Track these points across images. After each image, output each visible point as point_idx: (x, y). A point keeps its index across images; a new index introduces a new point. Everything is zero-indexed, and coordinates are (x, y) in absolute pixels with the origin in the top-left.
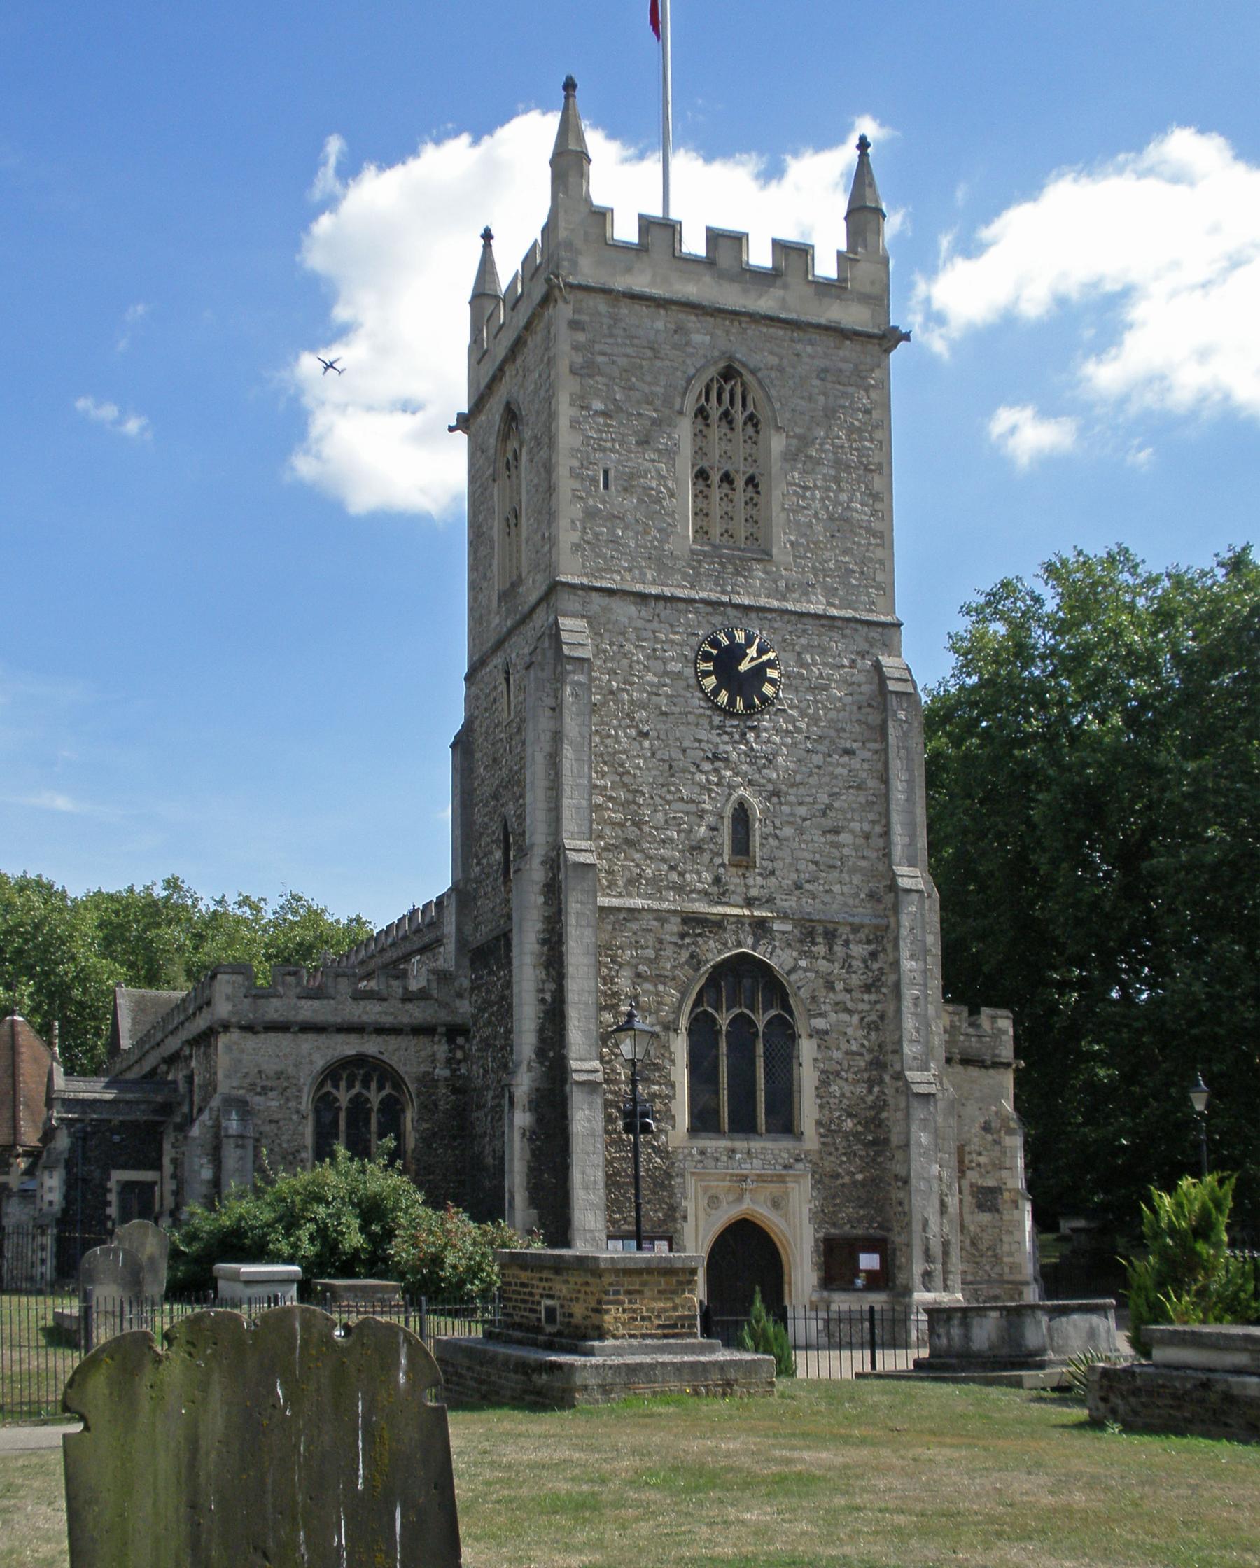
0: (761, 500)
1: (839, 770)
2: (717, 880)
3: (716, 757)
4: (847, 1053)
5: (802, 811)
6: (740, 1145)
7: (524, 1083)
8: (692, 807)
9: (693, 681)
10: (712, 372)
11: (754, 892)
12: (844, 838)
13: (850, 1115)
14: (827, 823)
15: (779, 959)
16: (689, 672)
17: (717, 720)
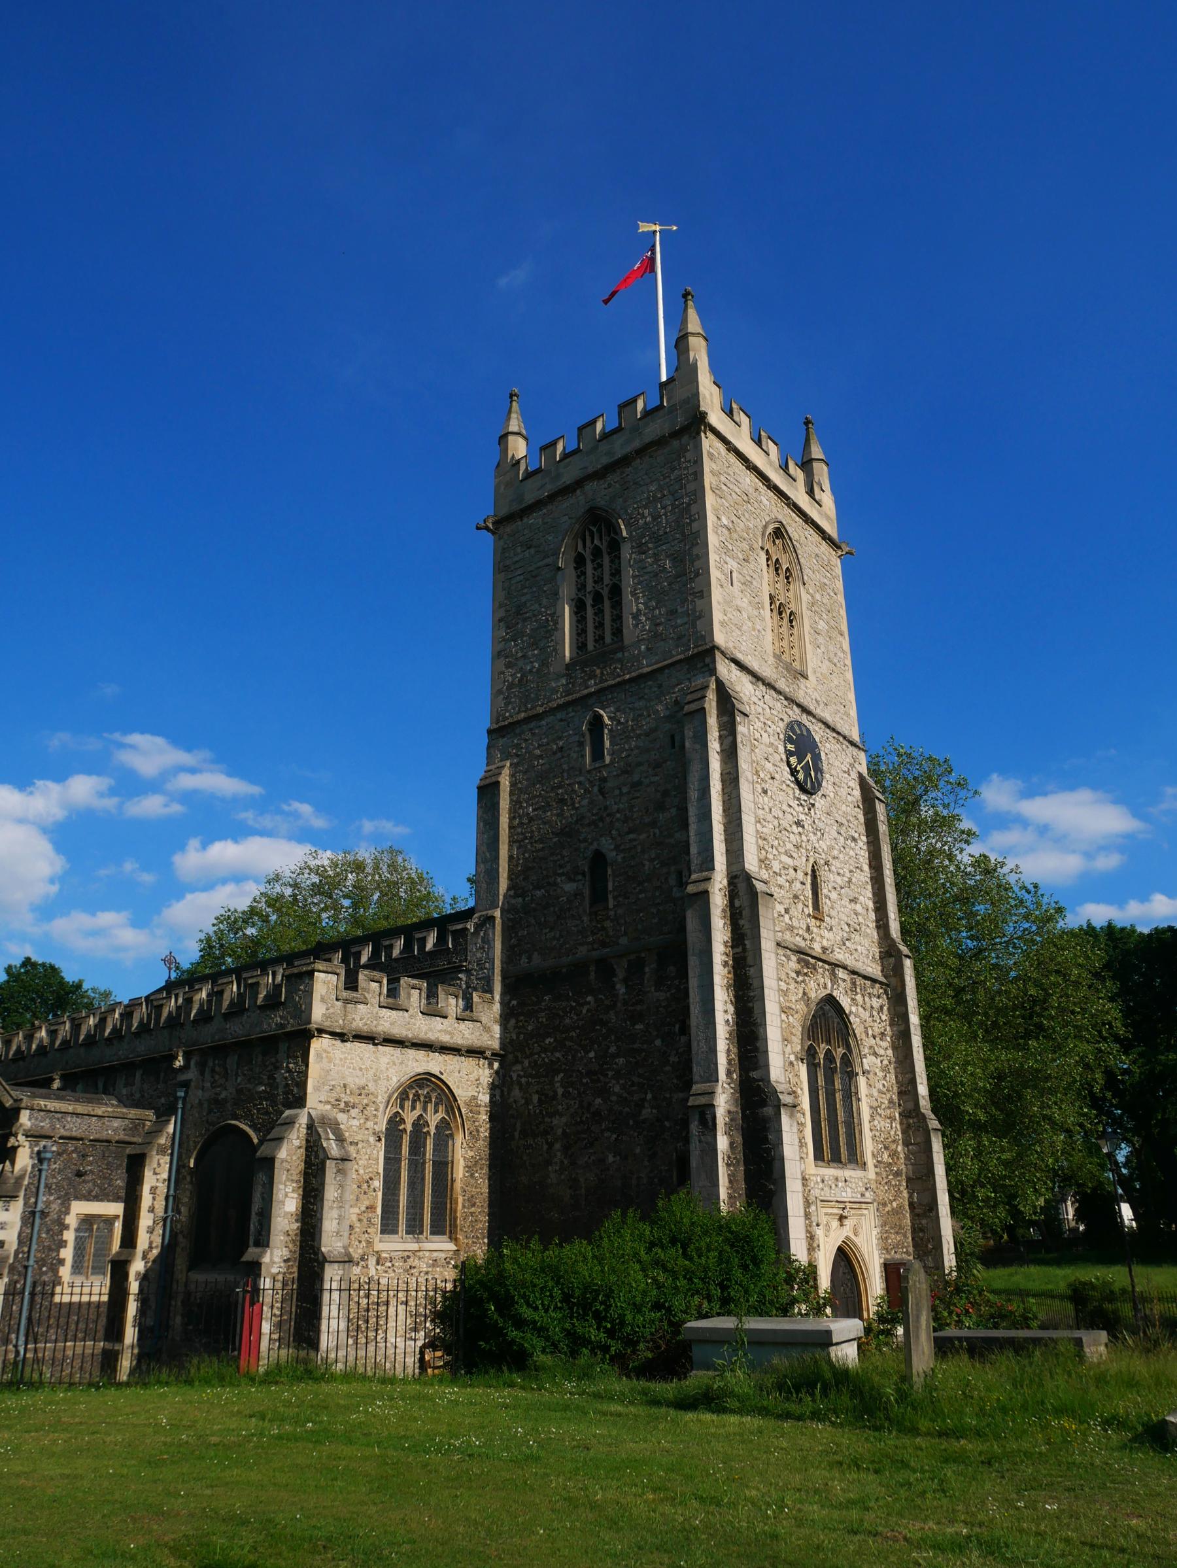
0: (795, 631)
1: (852, 853)
2: (808, 929)
3: (799, 823)
4: (880, 1092)
5: (839, 880)
6: (838, 1173)
7: (723, 1102)
8: (789, 861)
9: (784, 757)
10: (770, 530)
11: (825, 943)
12: (858, 907)
13: (886, 1148)
14: (852, 895)
15: (845, 1002)
16: (781, 749)
17: (797, 792)
